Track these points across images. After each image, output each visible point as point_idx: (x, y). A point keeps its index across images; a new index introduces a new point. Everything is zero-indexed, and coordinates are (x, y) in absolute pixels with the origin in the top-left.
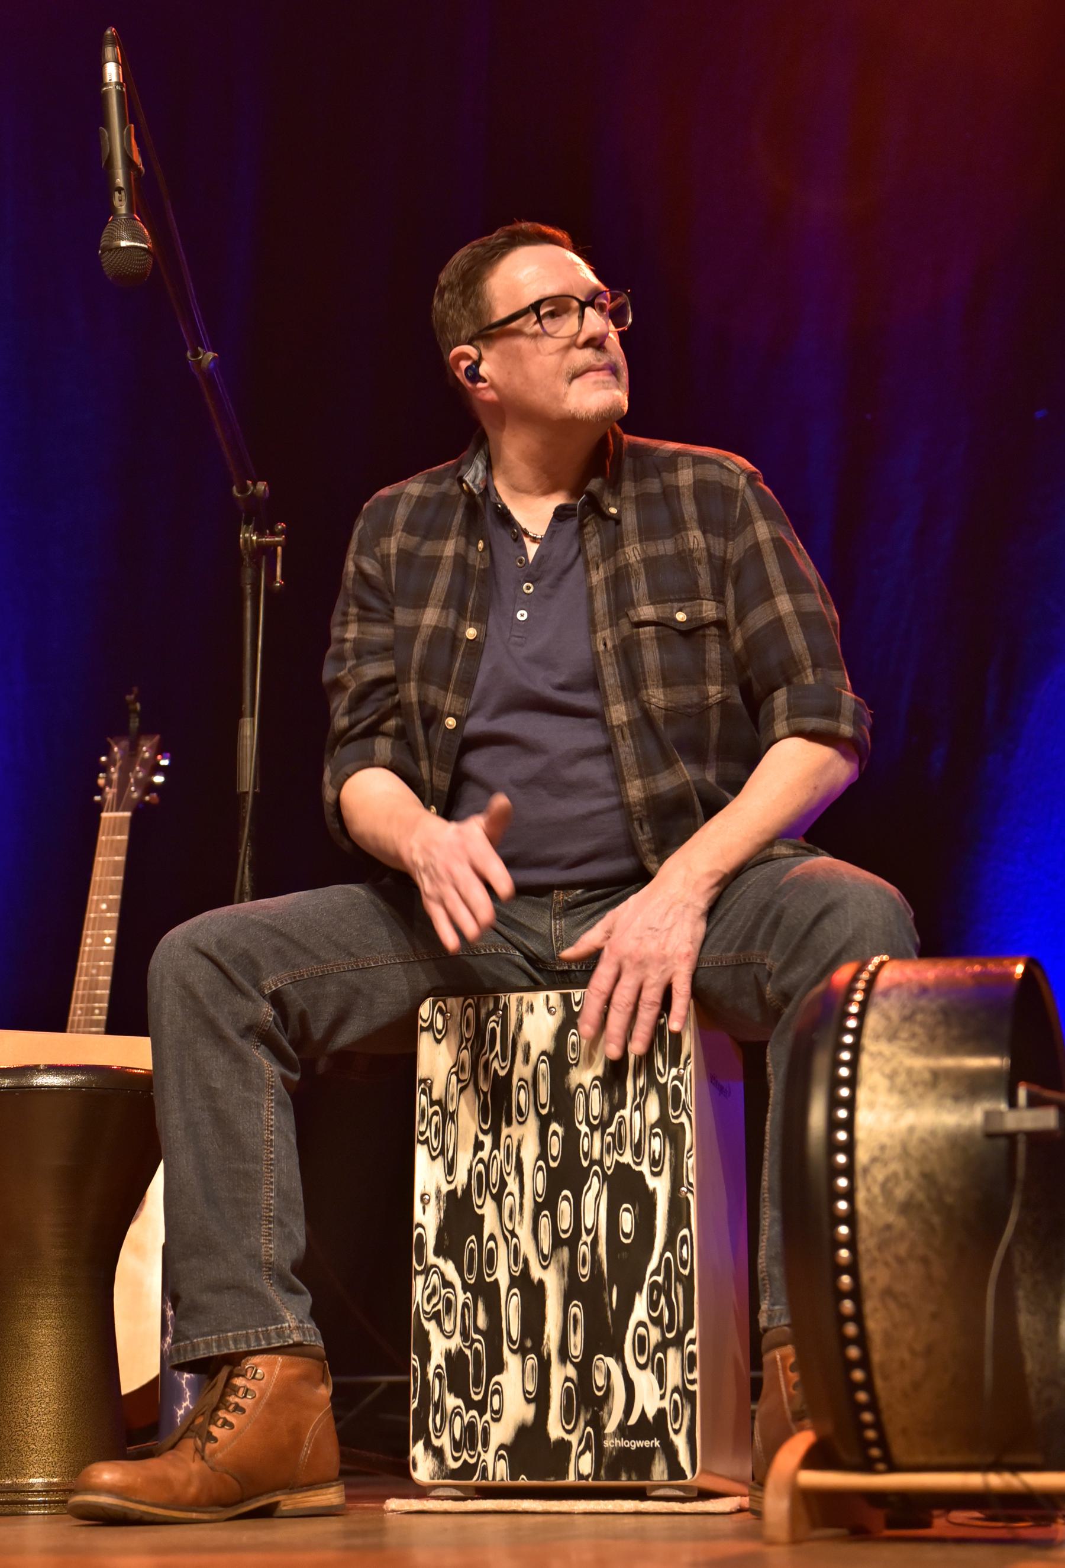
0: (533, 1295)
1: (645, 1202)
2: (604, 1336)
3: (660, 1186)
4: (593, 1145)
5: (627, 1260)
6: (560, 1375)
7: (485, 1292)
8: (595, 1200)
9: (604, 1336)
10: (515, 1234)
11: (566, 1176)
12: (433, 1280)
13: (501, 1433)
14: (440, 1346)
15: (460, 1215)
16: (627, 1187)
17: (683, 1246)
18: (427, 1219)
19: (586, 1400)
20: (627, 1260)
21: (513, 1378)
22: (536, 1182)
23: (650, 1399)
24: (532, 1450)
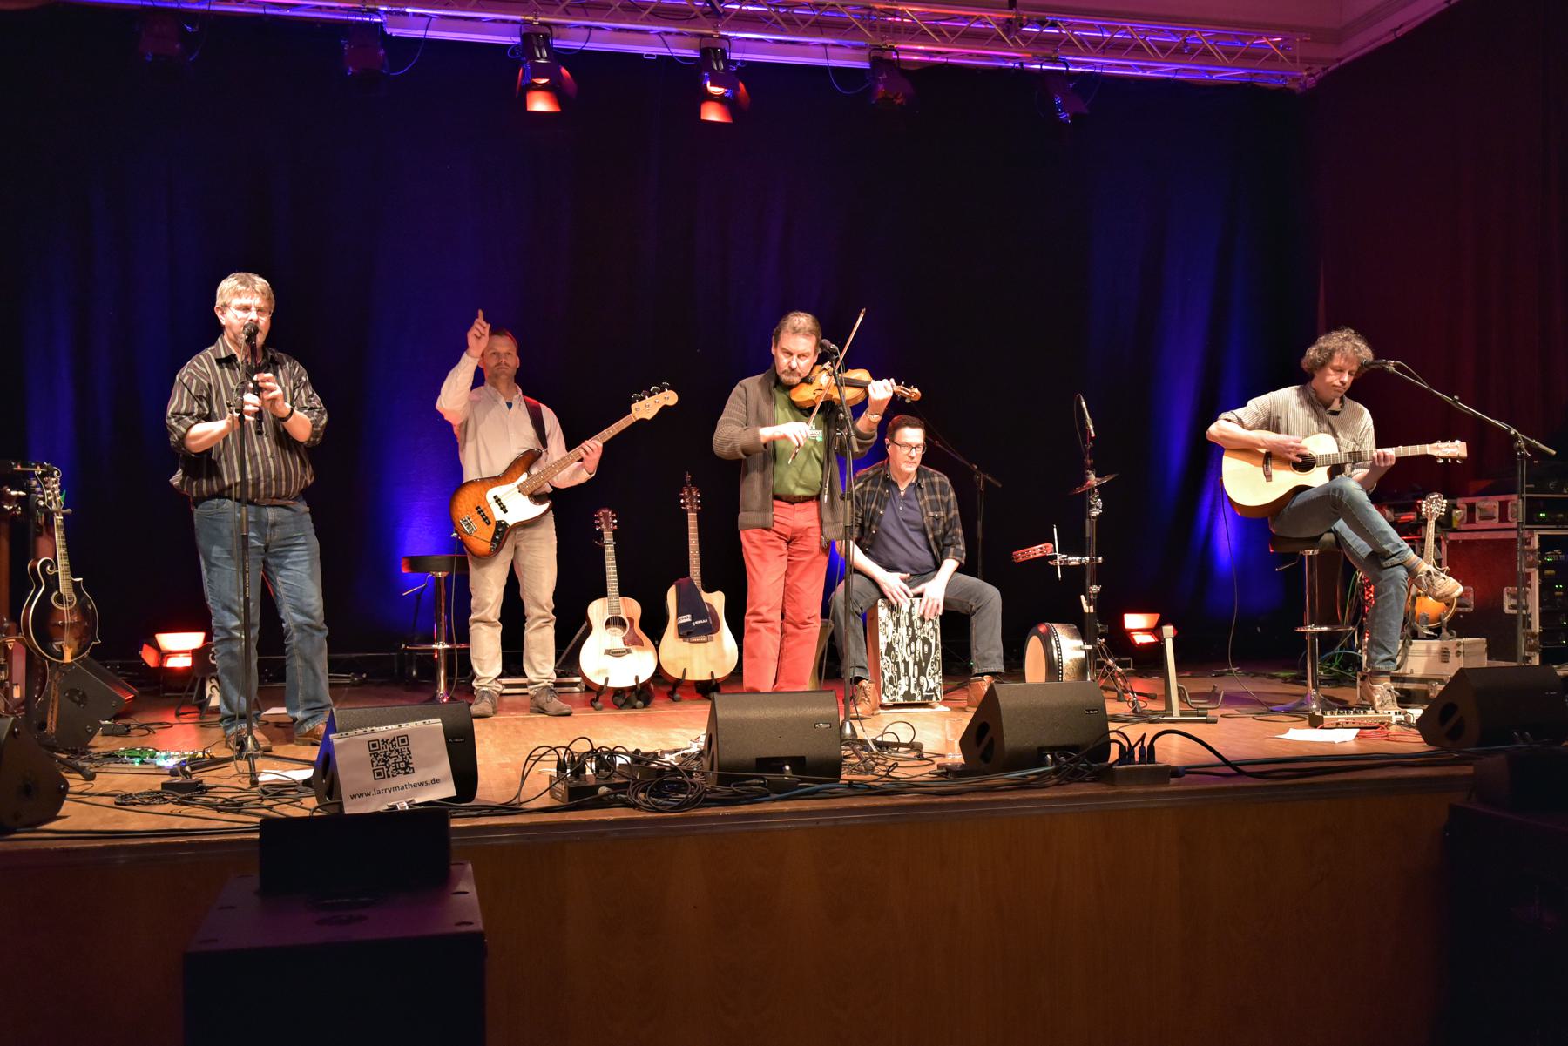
0: (907, 664)
1: (930, 645)
2: (922, 672)
3: (933, 641)
4: (918, 632)
5: (926, 657)
6: (913, 681)
7: (896, 663)
8: (919, 643)
9: (922, 672)
10: (902, 651)
11: (913, 639)
12: (885, 662)
13: (902, 692)
14: (887, 675)
15: (890, 648)
16: (926, 641)
17: (937, 655)
18: (883, 648)
19: (919, 685)
20: (926, 657)
21: (903, 681)
22: (906, 640)
23: (932, 685)
24: (907, 695)
